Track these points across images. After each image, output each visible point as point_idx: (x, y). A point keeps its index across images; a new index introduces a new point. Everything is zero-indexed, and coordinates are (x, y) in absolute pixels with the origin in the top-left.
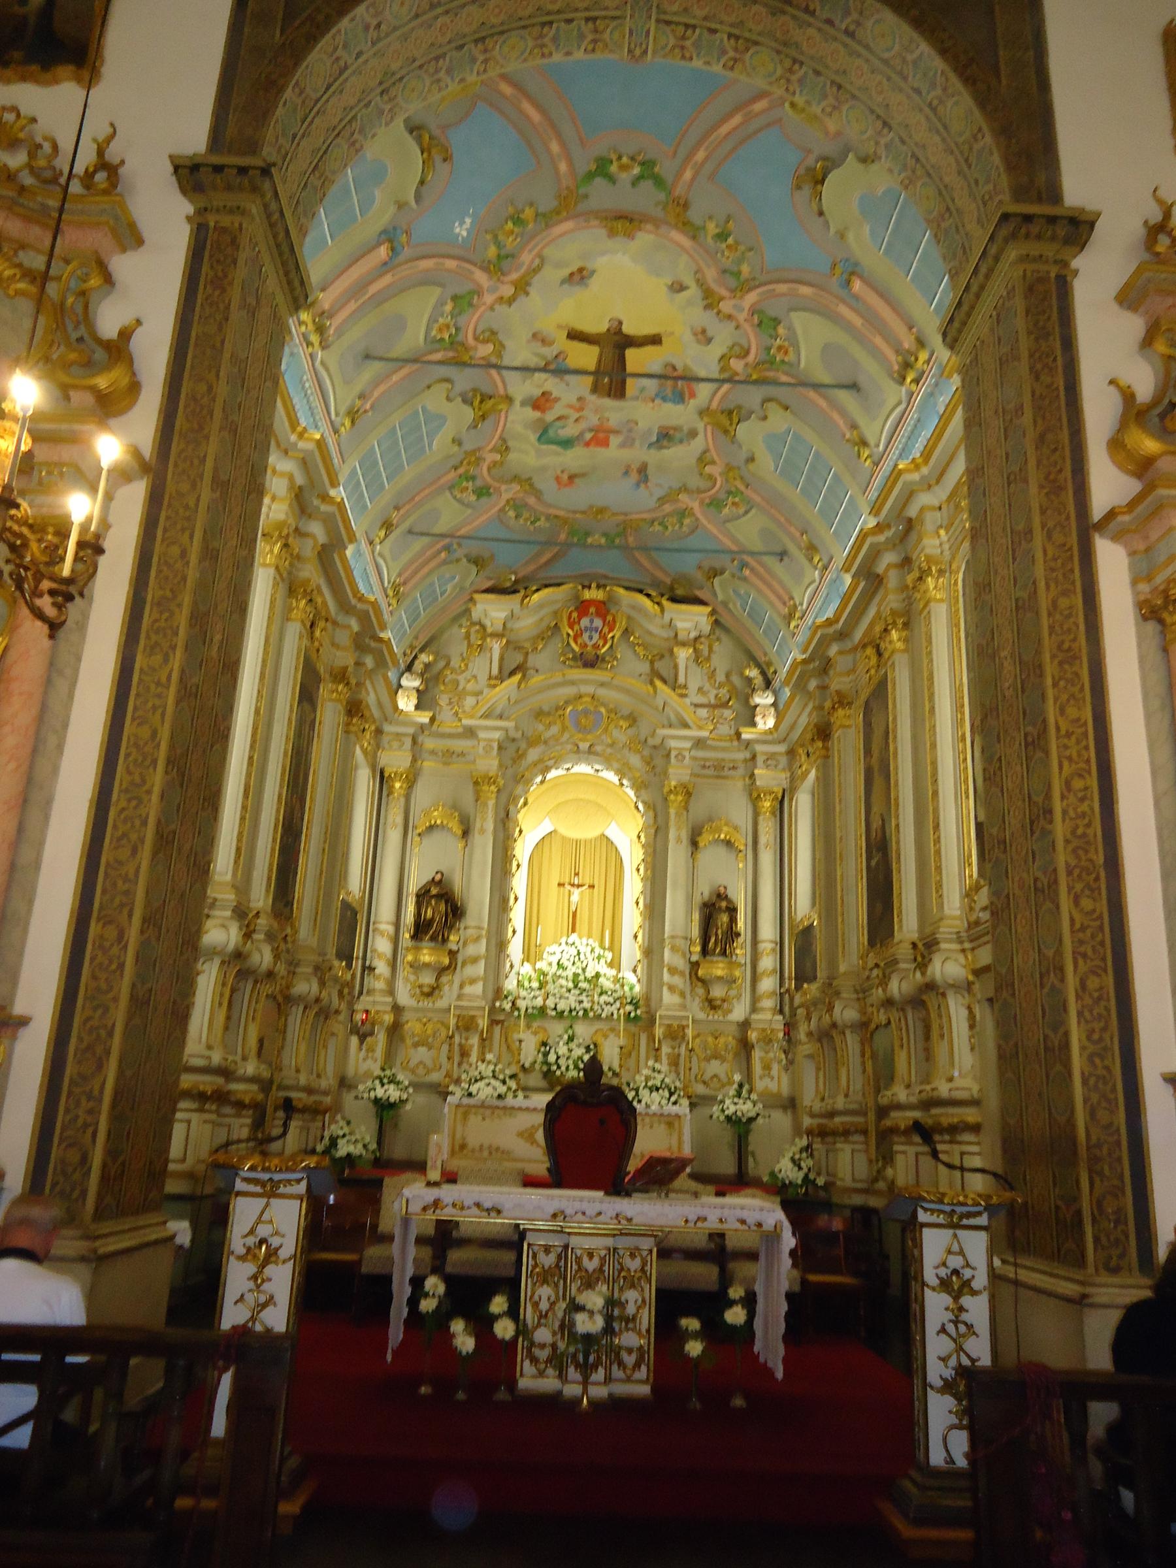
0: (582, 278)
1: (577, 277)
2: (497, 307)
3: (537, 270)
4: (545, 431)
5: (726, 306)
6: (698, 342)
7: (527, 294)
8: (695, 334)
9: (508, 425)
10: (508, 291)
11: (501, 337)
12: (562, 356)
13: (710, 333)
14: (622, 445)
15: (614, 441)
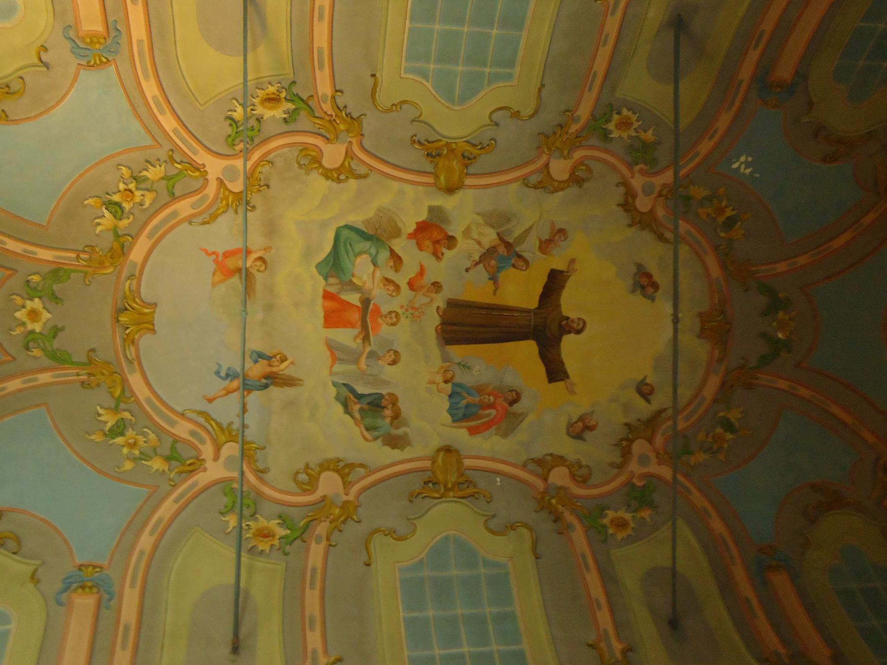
0: (643, 287)
1: (644, 281)
2: (622, 190)
3: (661, 238)
4: (363, 235)
5: (639, 447)
6: (570, 425)
7: (630, 226)
8: (581, 419)
9: (395, 185)
10: (643, 204)
11: (573, 190)
12: (521, 263)
13: (588, 435)
14: (332, 347)
15: (346, 337)
